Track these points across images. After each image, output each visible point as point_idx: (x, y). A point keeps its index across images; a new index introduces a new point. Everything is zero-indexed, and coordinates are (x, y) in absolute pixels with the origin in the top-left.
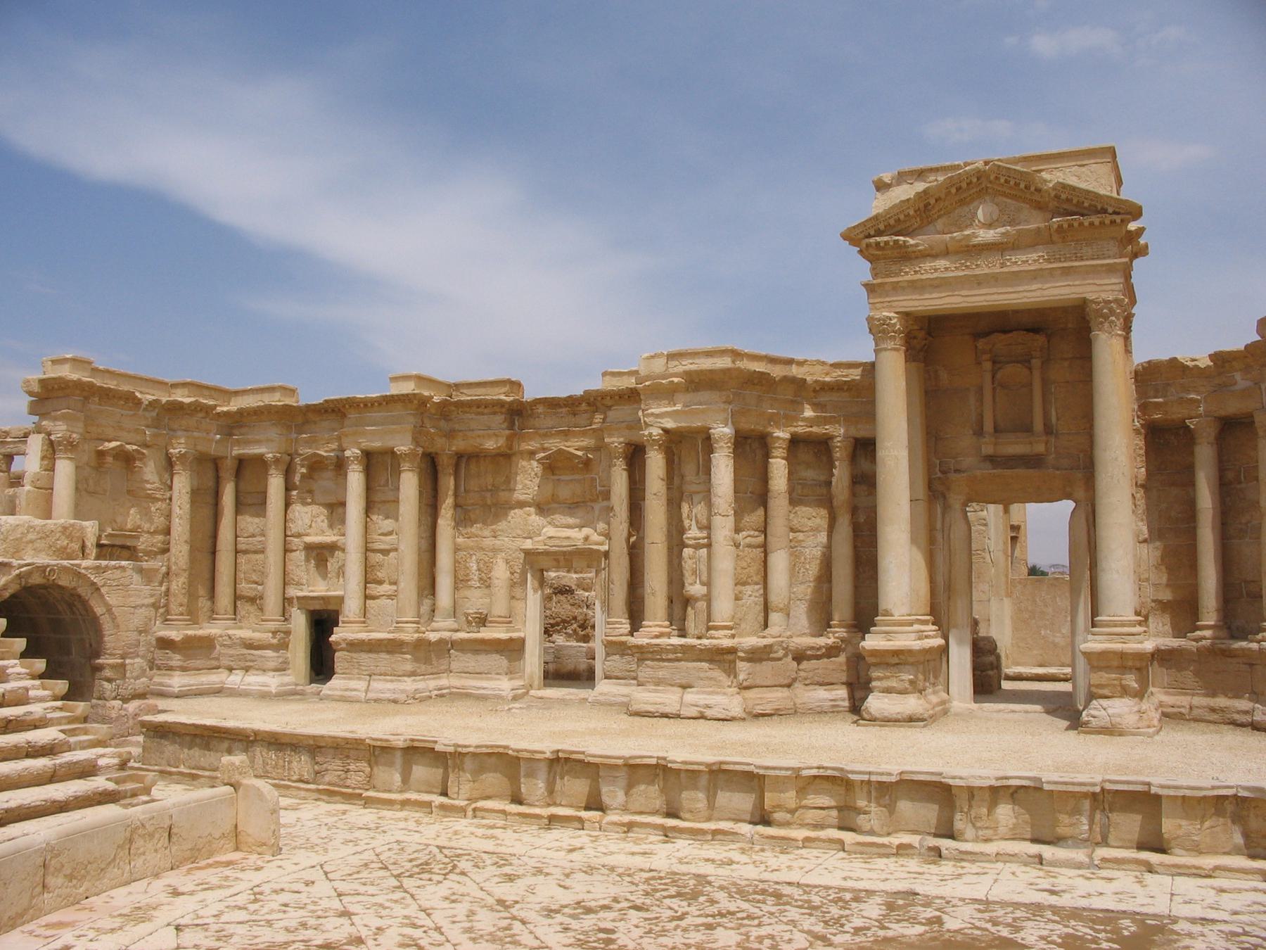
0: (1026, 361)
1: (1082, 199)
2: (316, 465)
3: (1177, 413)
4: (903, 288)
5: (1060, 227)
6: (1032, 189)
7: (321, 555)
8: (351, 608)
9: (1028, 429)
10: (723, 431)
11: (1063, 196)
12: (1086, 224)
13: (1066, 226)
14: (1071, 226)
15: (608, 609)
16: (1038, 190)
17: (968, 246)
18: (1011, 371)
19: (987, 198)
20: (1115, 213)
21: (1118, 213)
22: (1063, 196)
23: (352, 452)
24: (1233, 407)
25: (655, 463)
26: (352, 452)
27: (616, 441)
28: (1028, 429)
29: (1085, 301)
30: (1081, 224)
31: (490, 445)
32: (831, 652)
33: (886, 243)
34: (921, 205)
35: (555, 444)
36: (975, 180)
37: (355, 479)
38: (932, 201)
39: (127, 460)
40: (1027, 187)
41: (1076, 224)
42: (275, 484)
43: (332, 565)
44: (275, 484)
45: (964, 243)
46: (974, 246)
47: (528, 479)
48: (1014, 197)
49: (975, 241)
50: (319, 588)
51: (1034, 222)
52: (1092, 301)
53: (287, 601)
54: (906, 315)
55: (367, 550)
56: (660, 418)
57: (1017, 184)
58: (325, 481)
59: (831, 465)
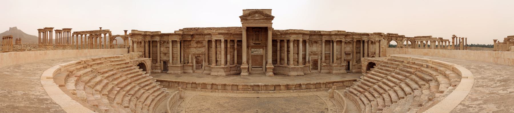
0: (259, 32)
2: (164, 42)
3: (276, 39)
7: (165, 54)
8: (171, 61)
9: (259, 40)
10: (223, 40)
15: (205, 61)
18: (257, 33)
23: (170, 41)
24: (282, 39)
25: (214, 44)
26: (170, 41)
27: (207, 40)
28: (259, 40)
31: (189, 40)
32: (235, 67)
35: (198, 40)
37: (171, 44)
39: (141, 42)
42: (159, 45)
43: (167, 55)
44: (159, 45)
47: (193, 44)
50: (165, 58)
51: (262, 17)
53: (160, 60)
55: (173, 54)
56: (214, 38)
58: (165, 44)
59: (234, 43)
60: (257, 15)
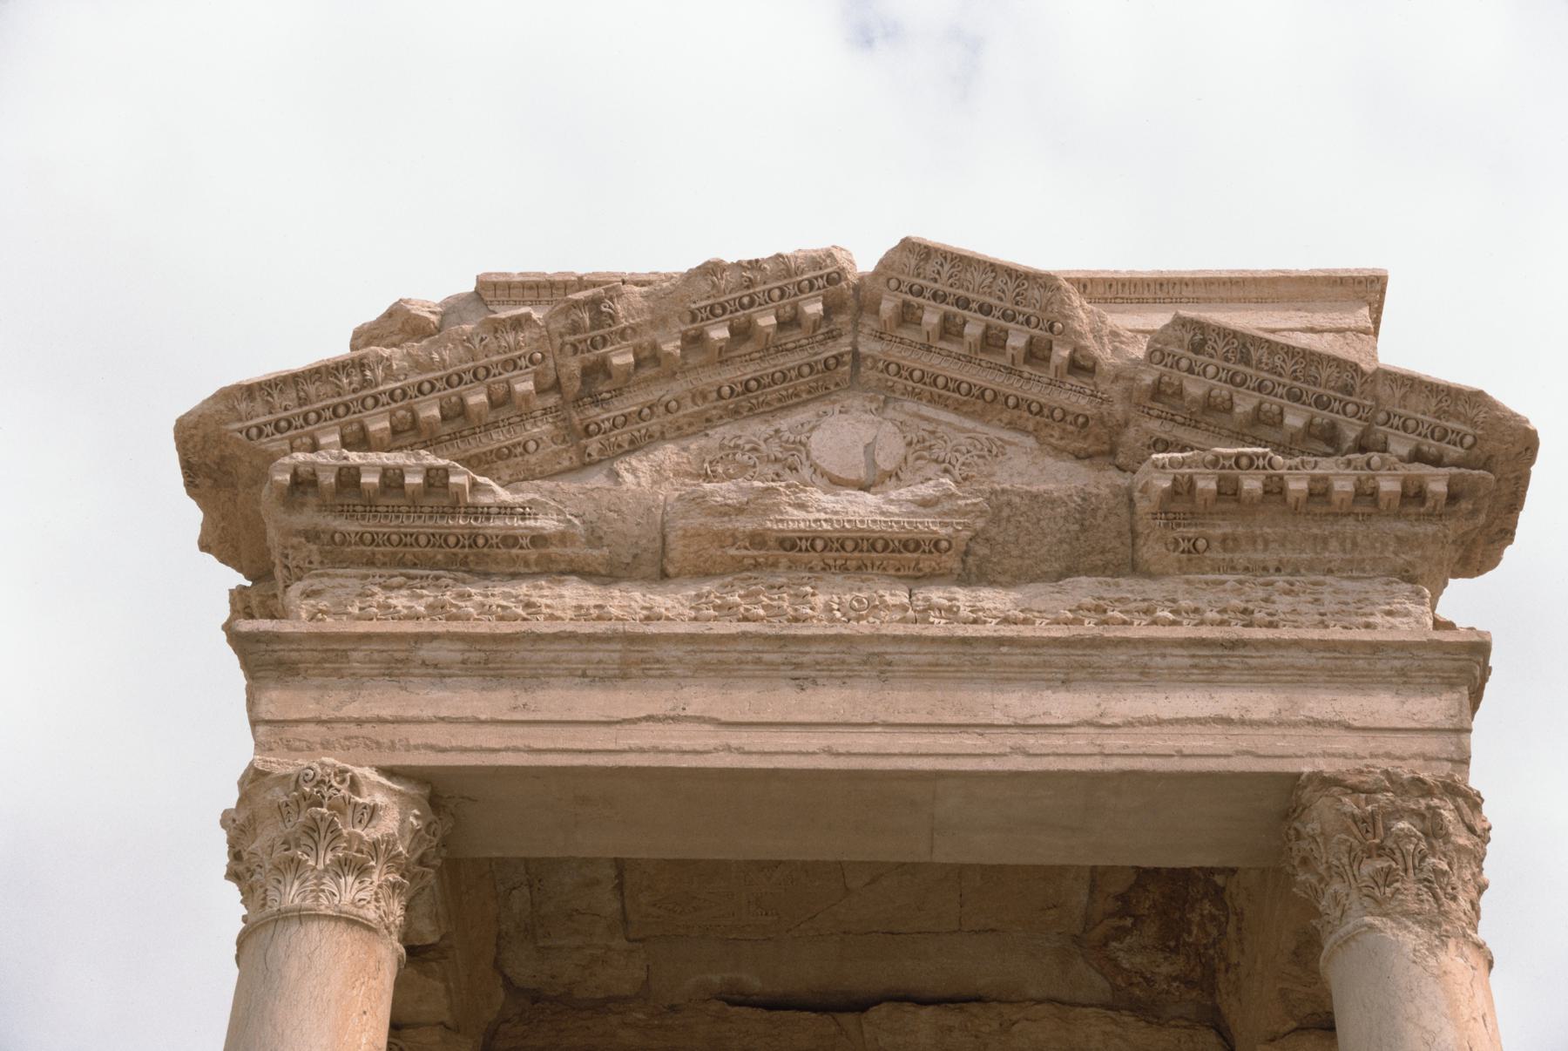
1: (1271, 404)
4: (438, 673)
5: (1183, 490)
6: (1062, 353)
11: (1195, 389)
12: (1297, 486)
13: (1207, 484)
14: (1229, 492)
16: (1081, 366)
17: (757, 540)
19: (856, 402)
20: (1417, 456)
21: (1437, 462)
22: (1195, 389)
29: (1287, 797)
30: (1275, 490)
33: (392, 480)
34: (574, 365)
36: (814, 308)
38: (622, 359)
40: (1036, 354)
41: (1252, 484)
45: (745, 524)
46: (789, 543)
48: (976, 402)
49: (796, 520)
52: (1325, 782)
54: (437, 791)
57: (992, 341)
60: (842, 433)
